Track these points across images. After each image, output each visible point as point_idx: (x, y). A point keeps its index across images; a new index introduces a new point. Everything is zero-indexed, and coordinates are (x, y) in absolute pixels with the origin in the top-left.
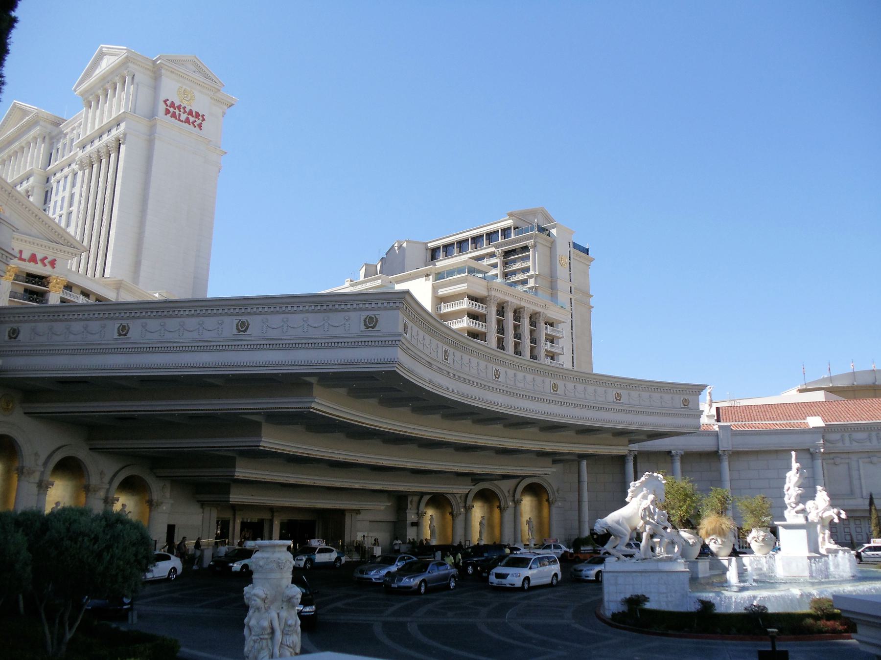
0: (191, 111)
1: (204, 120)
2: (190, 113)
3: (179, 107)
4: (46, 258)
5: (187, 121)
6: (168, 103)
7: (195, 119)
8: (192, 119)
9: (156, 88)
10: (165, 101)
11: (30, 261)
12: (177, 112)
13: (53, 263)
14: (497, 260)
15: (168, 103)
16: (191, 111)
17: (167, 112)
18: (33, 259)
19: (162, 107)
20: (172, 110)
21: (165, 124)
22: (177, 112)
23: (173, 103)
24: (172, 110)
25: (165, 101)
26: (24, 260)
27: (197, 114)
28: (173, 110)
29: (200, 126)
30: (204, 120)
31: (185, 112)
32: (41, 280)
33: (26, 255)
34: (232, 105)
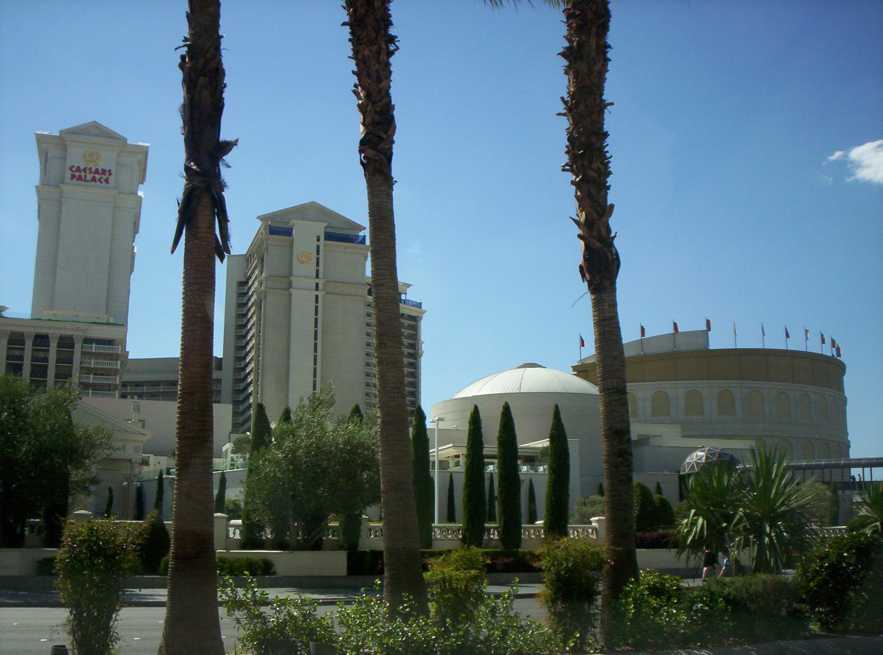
2: (97, 171)
3: (85, 170)
5: (94, 179)
6: (74, 169)
7: (101, 176)
8: (97, 176)
10: (71, 169)
12: (83, 174)
15: (74, 169)
17: (73, 177)
19: (68, 174)
21: (74, 189)
22: (83, 174)
24: (77, 174)
25: (71, 169)
27: (104, 172)
28: (78, 175)
29: (107, 181)
30: (110, 174)
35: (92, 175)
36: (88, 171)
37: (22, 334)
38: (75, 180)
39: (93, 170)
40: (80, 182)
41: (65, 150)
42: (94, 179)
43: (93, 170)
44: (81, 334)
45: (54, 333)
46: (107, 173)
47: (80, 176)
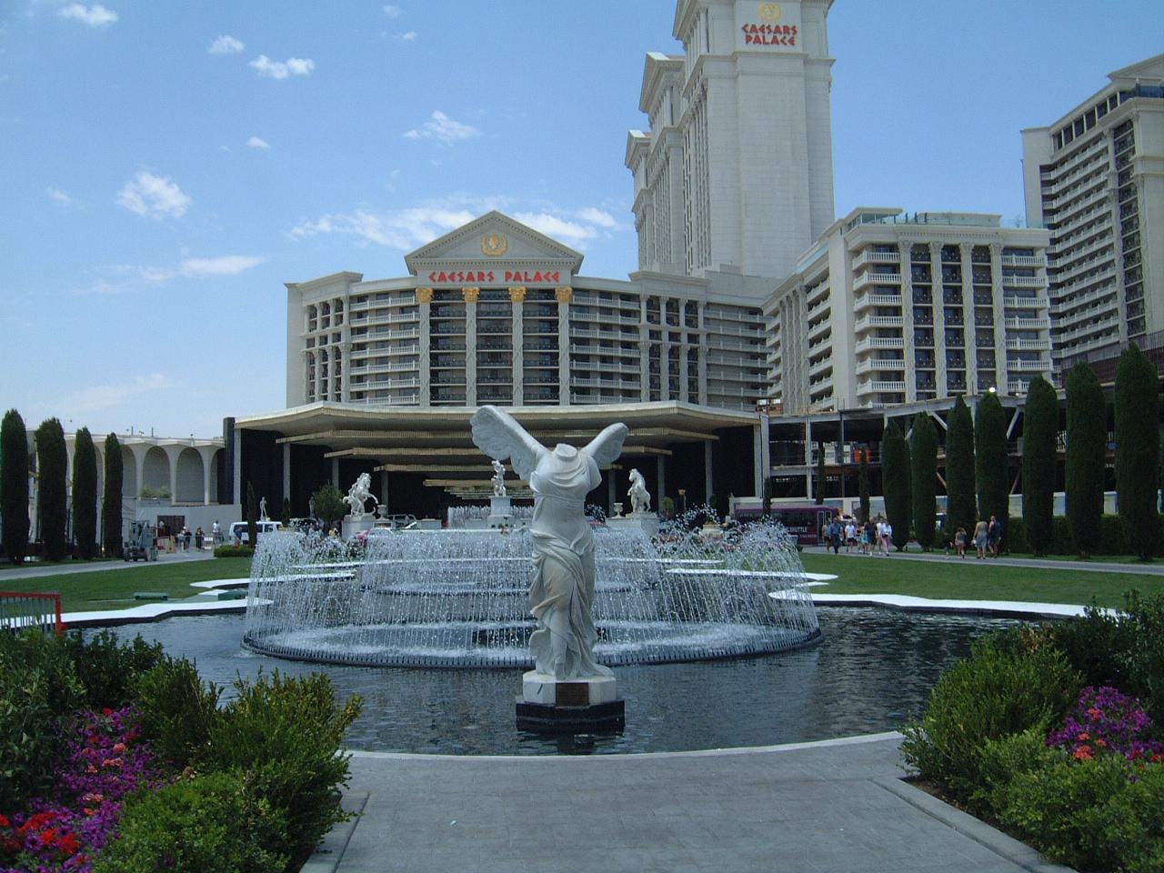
0: (777, 27)
1: (795, 32)
3: (762, 29)
4: (549, 273)
5: (775, 41)
6: (749, 29)
9: (732, 17)
10: (744, 29)
11: (534, 280)
13: (556, 277)
14: (1109, 143)
15: (749, 29)
16: (777, 27)
17: (748, 39)
18: (538, 277)
20: (753, 35)
22: (760, 35)
23: (754, 26)
25: (744, 29)
26: (530, 280)
27: (786, 29)
28: (753, 34)
29: (792, 42)
31: (770, 32)
32: (550, 293)
33: (532, 275)
36: (766, 31)
37: (926, 246)
39: (773, 28)
40: (758, 44)
42: (775, 41)
43: (773, 28)
46: (791, 32)
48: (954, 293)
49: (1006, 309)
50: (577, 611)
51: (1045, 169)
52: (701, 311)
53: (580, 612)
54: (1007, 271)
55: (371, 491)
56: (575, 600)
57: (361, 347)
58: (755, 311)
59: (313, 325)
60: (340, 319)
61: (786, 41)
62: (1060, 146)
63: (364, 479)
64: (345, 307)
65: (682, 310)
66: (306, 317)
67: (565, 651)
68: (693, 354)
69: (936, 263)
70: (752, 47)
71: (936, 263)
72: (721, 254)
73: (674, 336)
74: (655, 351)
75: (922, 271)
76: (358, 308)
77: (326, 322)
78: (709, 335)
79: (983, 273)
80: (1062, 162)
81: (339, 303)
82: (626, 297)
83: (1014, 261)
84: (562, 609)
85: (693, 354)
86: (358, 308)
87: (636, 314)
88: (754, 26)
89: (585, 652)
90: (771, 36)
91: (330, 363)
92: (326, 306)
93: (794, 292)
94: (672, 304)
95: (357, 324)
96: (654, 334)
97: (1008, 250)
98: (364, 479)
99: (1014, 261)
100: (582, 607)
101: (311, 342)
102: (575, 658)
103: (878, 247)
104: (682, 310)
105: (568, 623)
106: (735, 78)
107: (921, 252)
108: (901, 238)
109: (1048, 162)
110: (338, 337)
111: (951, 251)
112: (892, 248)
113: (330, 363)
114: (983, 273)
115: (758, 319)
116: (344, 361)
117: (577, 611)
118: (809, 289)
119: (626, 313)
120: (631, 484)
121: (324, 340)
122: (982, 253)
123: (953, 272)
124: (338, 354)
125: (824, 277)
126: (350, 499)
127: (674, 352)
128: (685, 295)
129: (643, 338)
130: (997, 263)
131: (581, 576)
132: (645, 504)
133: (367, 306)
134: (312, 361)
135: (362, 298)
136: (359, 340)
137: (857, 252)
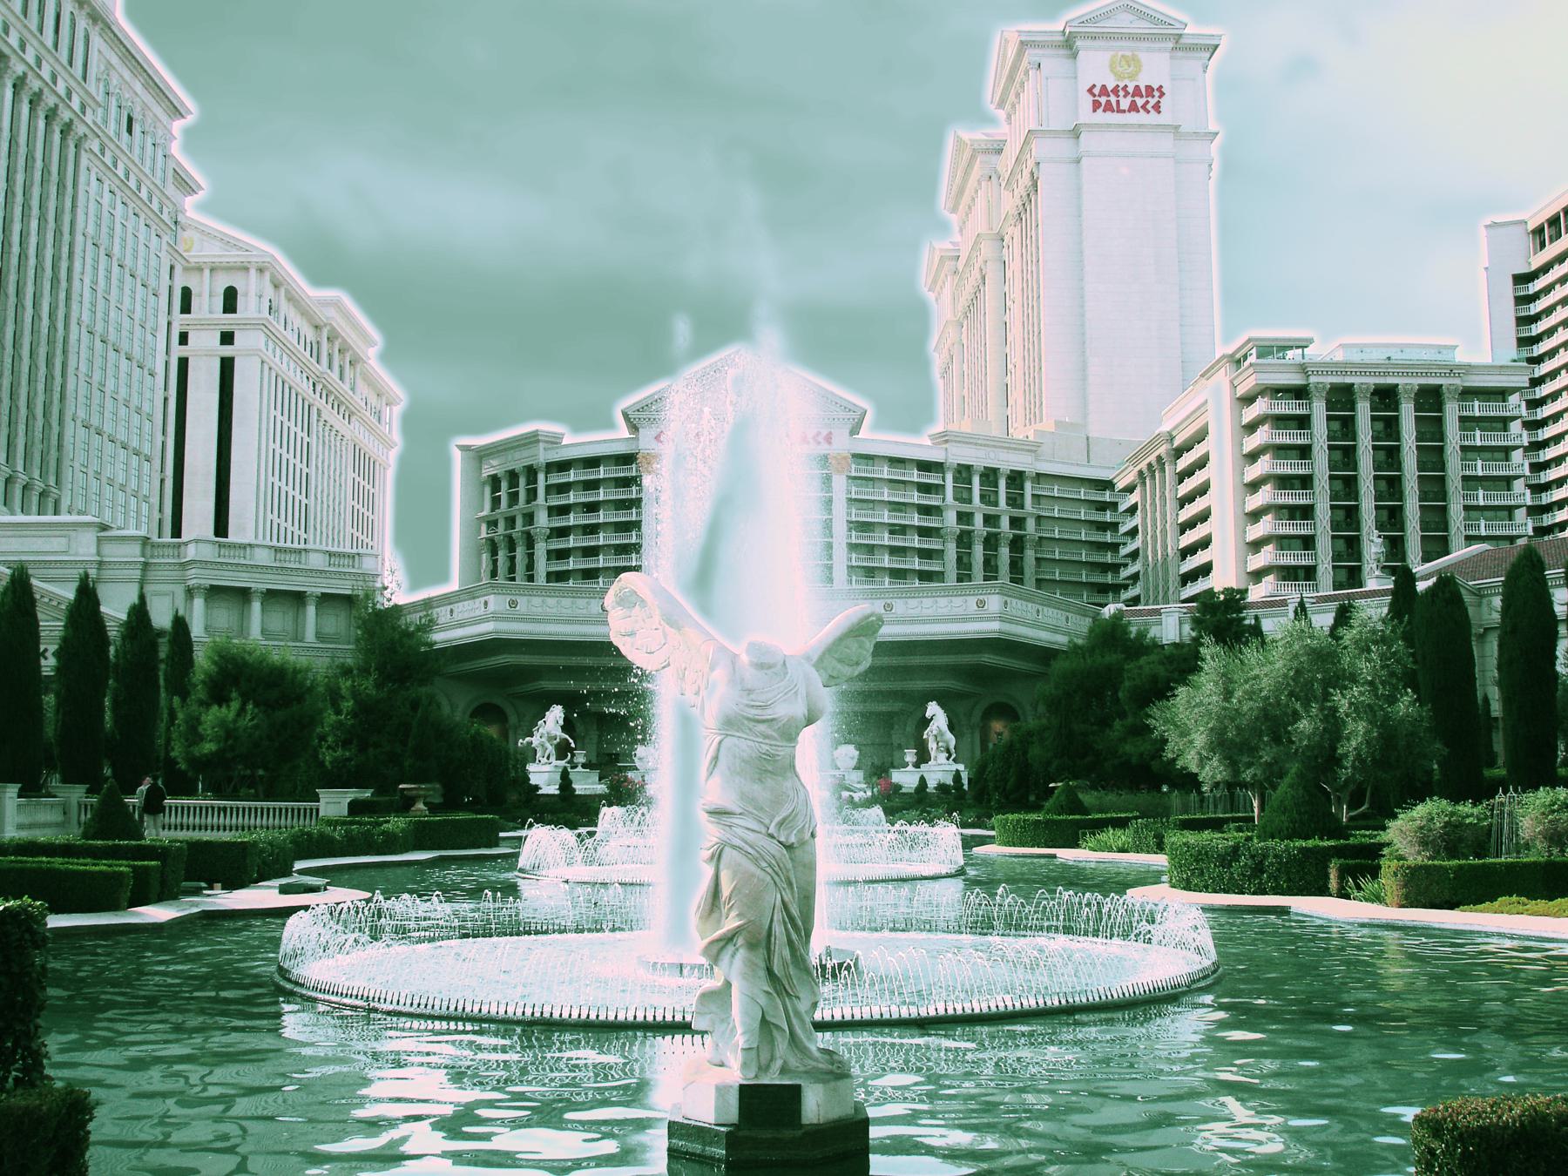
1: (1162, 95)
3: (1115, 91)
5: (1133, 108)
8: (1140, 102)
10: (1090, 91)
12: (1113, 99)
15: (1096, 91)
17: (1096, 105)
20: (1103, 100)
22: (1113, 99)
23: (1104, 87)
24: (1103, 100)
25: (1090, 91)
27: (1149, 89)
28: (1103, 99)
29: (1157, 107)
31: (1127, 94)
34: (1216, 47)
35: (1129, 99)
36: (1121, 93)
38: (1100, 111)
39: (1130, 90)
41: (1074, 56)
43: (1130, 90)
44: (1457, 381)
45: (1408, 383)
46: (1156, 94)
47: (1108, 102)
48: (1389, 456)
49: (1465, 478)
50: (781, 951)
51: (1522, 279)
52: (1028, 485)
53: (787, 953)
54: (1466, 422)
55: (564, 729)
56: (778, 929)
57: (563, 532)
58: (1107, 485)
59: (496, 502)
60: (532, 495)
61: (1149, 107)
62: (1543, 245)
63: (556, 714)
64: (541, 477)
65: (1002, 483)
66: (488, 490)
67: (757, 1024)
68: (1017, 544)
69: (1363, 412)
70: (1101, 117)
71: (1363, 412)
72: (1056, 408)
73: (990, 520)
74: (964, 540)
75: (1344, 426)
76: (556, 479)
77: (514, 498)
78: (1039, 518)
79: (1431, 428)
80: (1545, 269)
81: (531, 472)
82: (925, 466)
83: (1477, 409)
84: (752, 946)
85: (1017, 544)
86: (556, 479)
87: (939, 489)
88: (1104, 87)
89: (795, 1021)
90: (1129, 99)
91: (520, 552)
92: (513, 476)
93: (1159, 458)
94: (990, 475)
95: (557, 501)
96: (964, 517)
97: (1468, 393)
98: (556, 714)
99: (1477, 409)
100: (790, 942)
101: (492, 524)
102: (776, 1033)
103: (1277, 391)
104: (1002, 483)
105: (762, 973)
106: (1078, 161)
107: (1342, 397)
108: (1313, 379)
109: (1523, 269)
110: (529, 518)
111: (1386, 397)
112: (1300, 393)
113: (520, 552)
114: (1431, 428)
115: (1107, 497)
116: (541, 549)
117: (781, 951)
118: (1179, 453)
119: (925, 488)
120: (926, 722)
121: (511, 522)
122: (1430, 398)
123: (1389, 427)
124: (530, 542)
125: (1200, 436)
126: (536, 741)
127: (991, 542)
128: (1007, 461)
129: (950, 518)
130: (1452, 412)
131: (790, 884)
132: (948, 751)
133: (572, 476)
134: (494, 552)
135: (563, 466)
136: (559, 523)
137: (1248, 400)
